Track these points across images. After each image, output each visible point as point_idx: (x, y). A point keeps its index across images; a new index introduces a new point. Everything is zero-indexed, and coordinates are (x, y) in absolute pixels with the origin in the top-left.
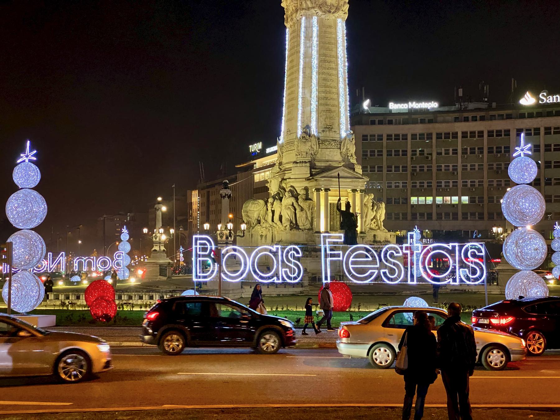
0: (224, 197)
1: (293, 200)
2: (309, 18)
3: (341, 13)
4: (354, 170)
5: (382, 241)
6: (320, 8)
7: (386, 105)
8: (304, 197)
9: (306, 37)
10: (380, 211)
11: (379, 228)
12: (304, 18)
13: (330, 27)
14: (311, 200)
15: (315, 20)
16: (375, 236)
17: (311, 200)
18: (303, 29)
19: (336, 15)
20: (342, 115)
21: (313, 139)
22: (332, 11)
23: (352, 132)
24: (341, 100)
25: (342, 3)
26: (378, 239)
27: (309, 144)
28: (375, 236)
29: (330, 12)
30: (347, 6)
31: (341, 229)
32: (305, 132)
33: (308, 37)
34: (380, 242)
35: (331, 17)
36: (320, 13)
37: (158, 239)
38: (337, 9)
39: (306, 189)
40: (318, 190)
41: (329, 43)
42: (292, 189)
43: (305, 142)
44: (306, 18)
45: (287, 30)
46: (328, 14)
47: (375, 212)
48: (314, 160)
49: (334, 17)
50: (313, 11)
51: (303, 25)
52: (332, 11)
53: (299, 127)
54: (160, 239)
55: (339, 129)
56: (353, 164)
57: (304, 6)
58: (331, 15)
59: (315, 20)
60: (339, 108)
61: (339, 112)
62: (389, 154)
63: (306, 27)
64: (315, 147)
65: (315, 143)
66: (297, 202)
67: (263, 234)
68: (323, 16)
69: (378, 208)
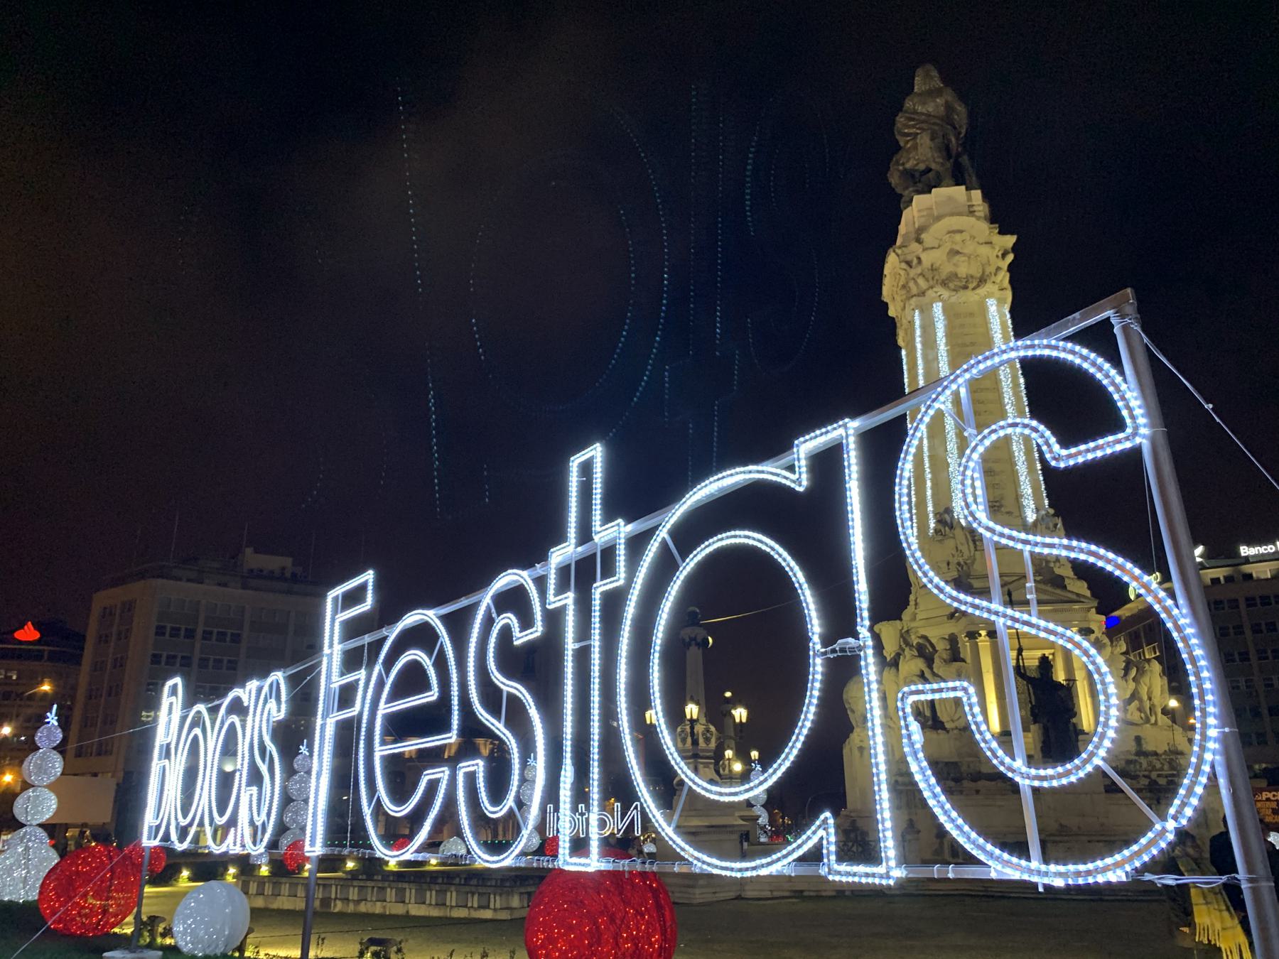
0: (689, 645)
1: (920, 664)
2: (926, 311)
3: (989, 287)
4: (1065, 587)
5: (1160, 751)
6: (944, 284)
7: (1237, 554)
8: (945, 656)
9: (924, 344)
10: (1146, 679)
11: (1147, 721)
12: (917, 312)
13: (972, 315)
14: (963, 661)
15: (938, 309)
16: (1138, 740)
17: (963, 661)
18: (918, 332)
19: (981, 291)
20: (1022, 478)
21: (958, 532)
22: (971, 286)
23: (1052, 511)
24: (1015, 448)
25: (992, 269)
26: (1149, 746)
27: (950, 543)
28: (1138, 740)
29: (966, 288)
30: (1004, 277)
31: (1035, 722)
32: (940, 521)
33: (930, 343)
34: (1155, 754)
35: (971, 297)
36: (945, 293)
37: (727, 771)
38: (982, 281)
39: (953, 640)
40: (973, 635)
41: (973, 344)
42: (921, 641)
43: (940, 541)
44: (922, 312)
45: (904, 353)
46: (962, 292)
47: (1132, 685)
48: (968, 576)
49: (977, 298)
50: (930, 293)
51: (917, 323)
52: (971, 286)
53: (931, 516)
54: (730, 771)
55: (1020, 508)
56: (1062, 578)
57: (914, 290)
58: (969, 293)
59: (938, 309)
60: (1013, 464)
61: (1015, 474)
62: (1256, 629)
63: (923, 327)
64: (964, 548)
65: (964, 541)
66: (930, 666)
67: (863, 745)
68: (953, 299)
69: (1141, 672)
